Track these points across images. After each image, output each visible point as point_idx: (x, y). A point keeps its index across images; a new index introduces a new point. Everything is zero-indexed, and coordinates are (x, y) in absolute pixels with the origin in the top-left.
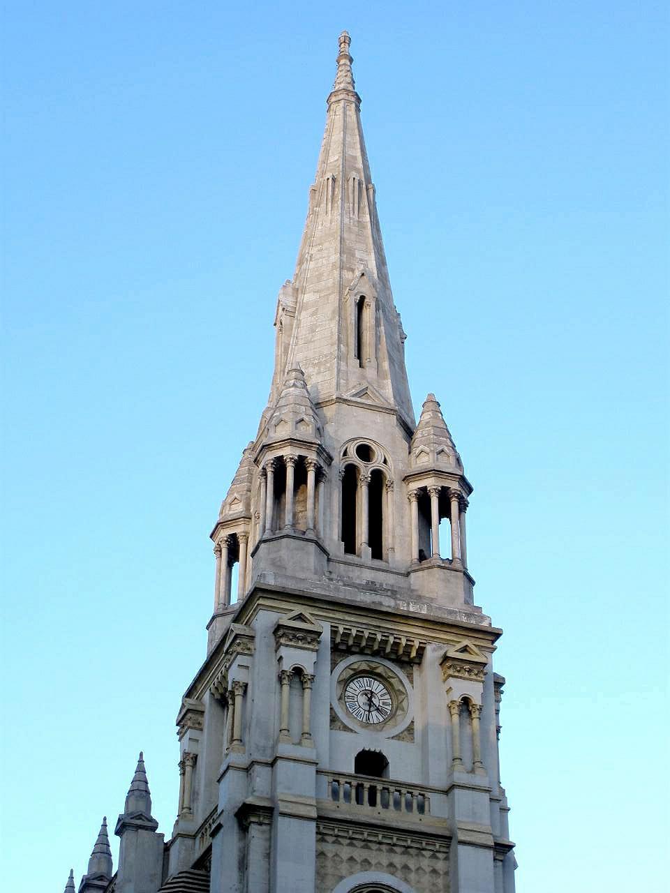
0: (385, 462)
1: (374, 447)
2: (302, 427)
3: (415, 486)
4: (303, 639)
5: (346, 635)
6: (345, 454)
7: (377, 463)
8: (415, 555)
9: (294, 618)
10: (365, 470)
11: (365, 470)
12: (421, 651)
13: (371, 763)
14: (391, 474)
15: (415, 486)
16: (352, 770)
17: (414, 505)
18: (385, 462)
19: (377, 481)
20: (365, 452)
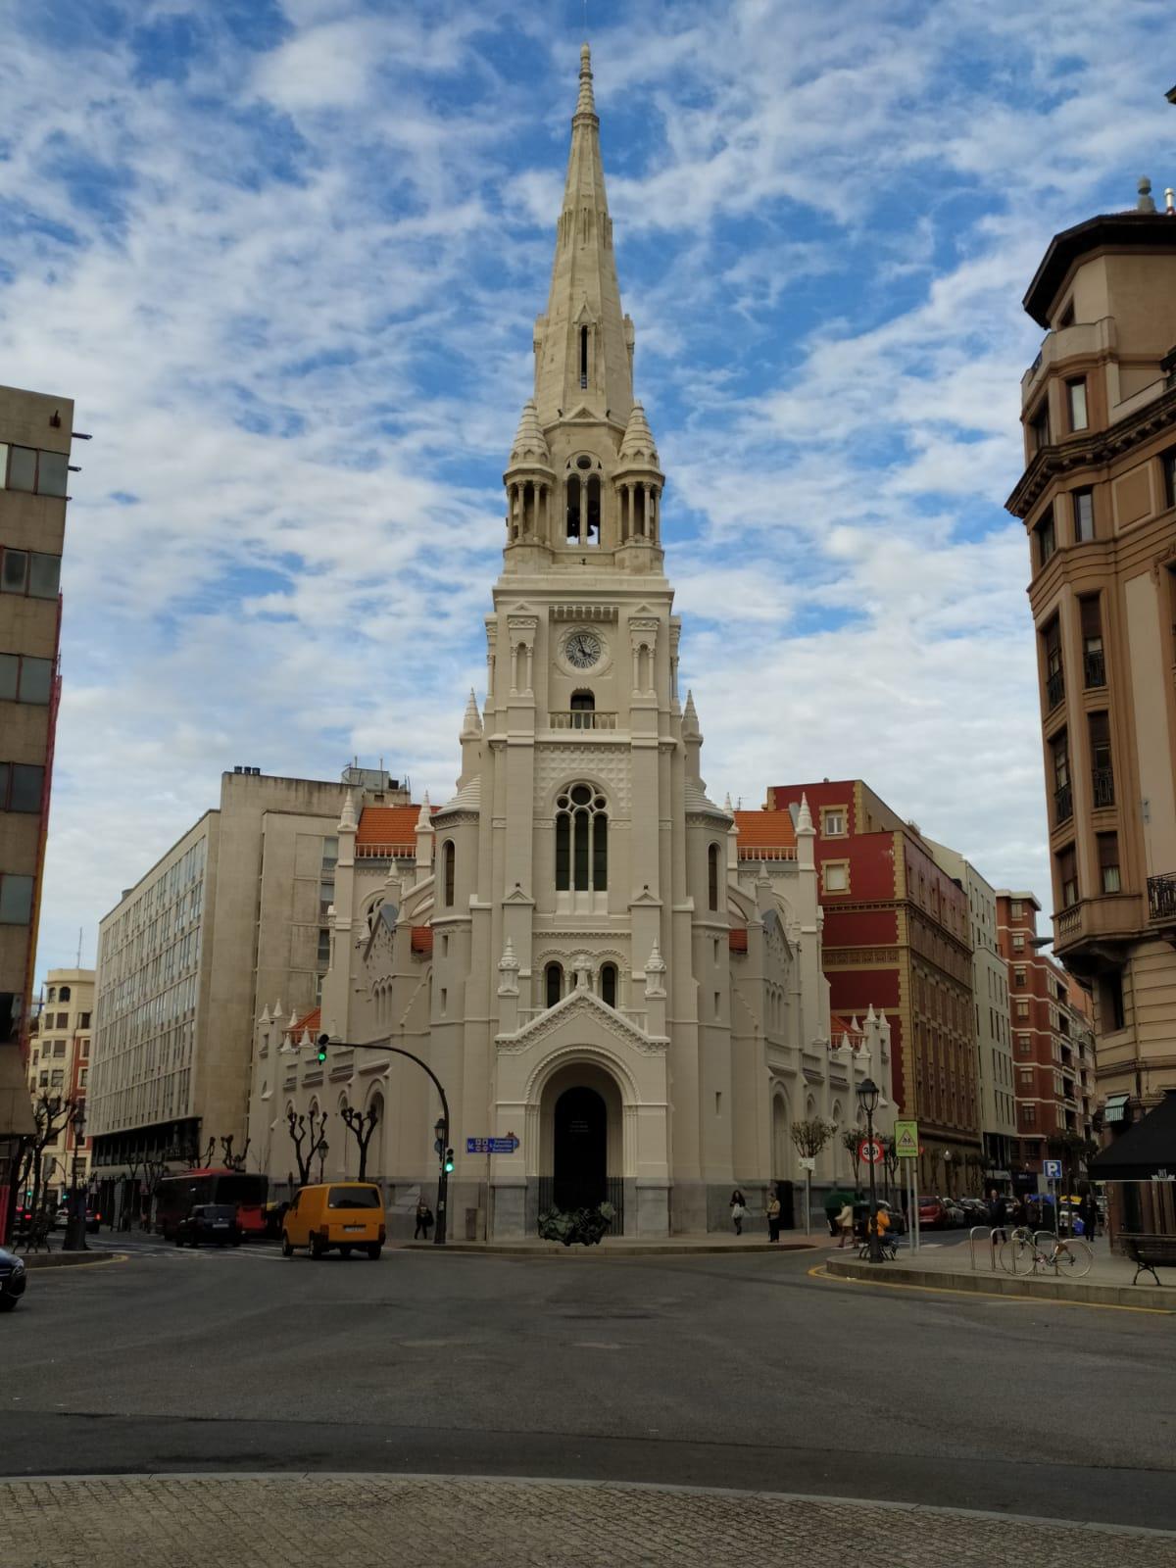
0: (600, 467)
1: (591, 456)
2: (530, 458)
3: (619, 483)
4: (522, 623)
5: (561, 612)
6: (569, 466)
7: (594, 469)
8: (620, 537)
9: (517, 609)
10: (584, 476)
11: (584, 476)
12: (616, 613)
13: (583, 699)
14: (604, 476)
15: (619, 483)
16: (567, 708)
17: (619, 499)
18: (600, 467)
19: (595, 484)
20: (584, 463)
